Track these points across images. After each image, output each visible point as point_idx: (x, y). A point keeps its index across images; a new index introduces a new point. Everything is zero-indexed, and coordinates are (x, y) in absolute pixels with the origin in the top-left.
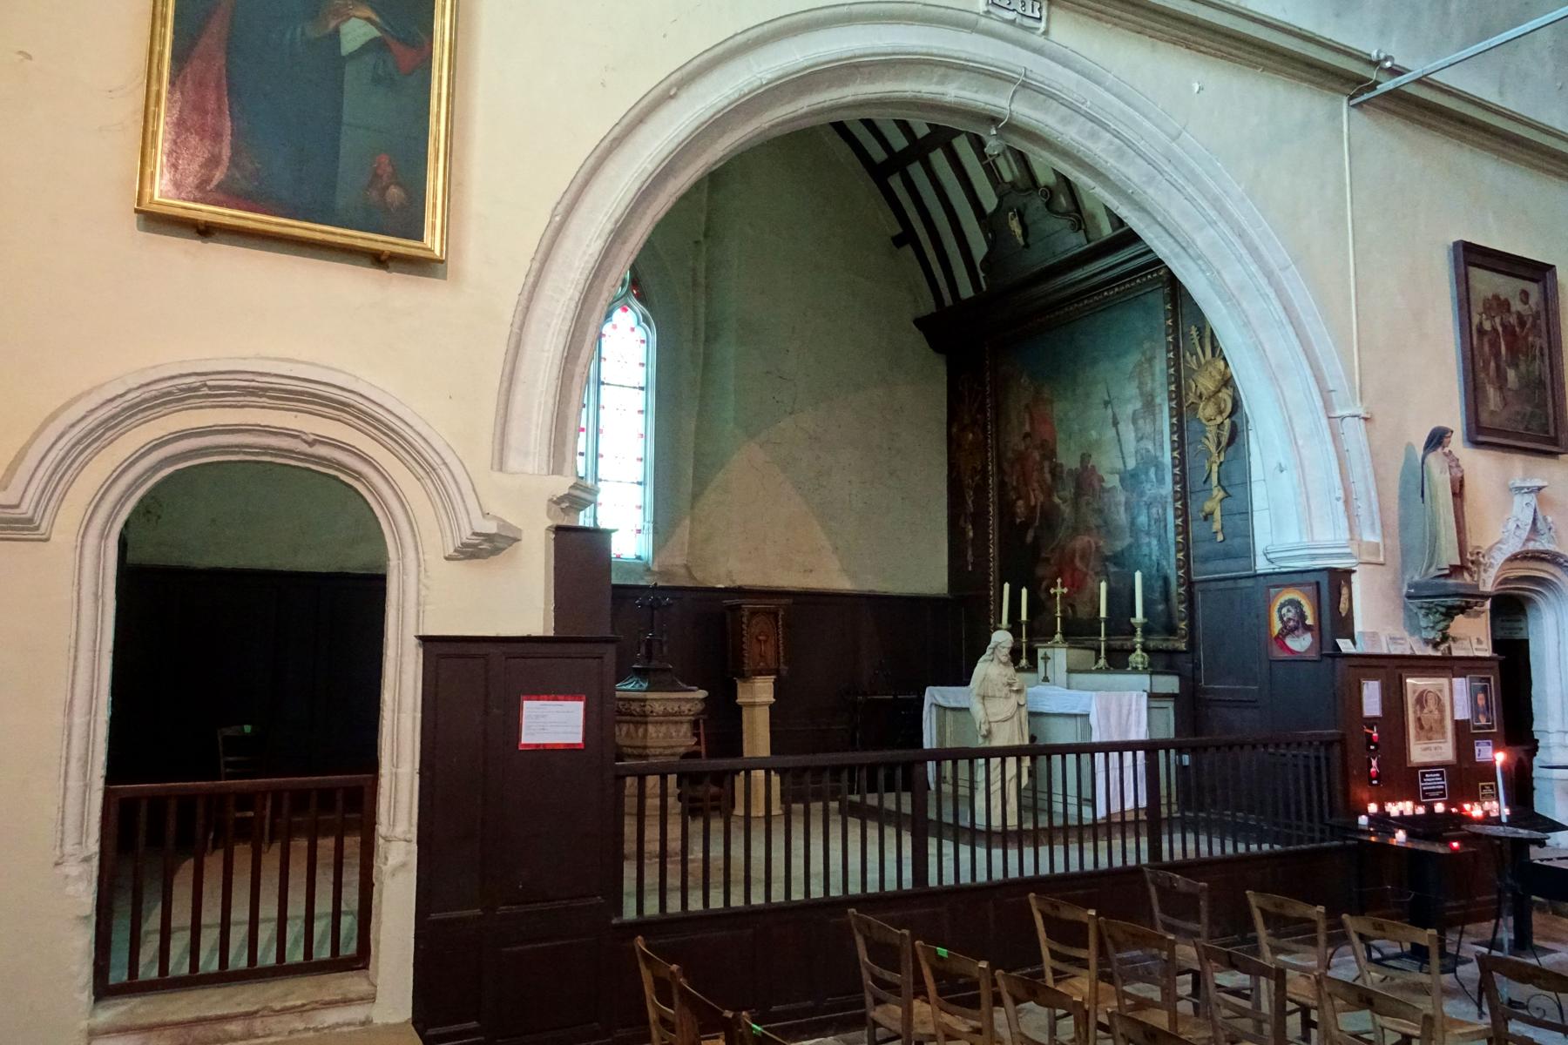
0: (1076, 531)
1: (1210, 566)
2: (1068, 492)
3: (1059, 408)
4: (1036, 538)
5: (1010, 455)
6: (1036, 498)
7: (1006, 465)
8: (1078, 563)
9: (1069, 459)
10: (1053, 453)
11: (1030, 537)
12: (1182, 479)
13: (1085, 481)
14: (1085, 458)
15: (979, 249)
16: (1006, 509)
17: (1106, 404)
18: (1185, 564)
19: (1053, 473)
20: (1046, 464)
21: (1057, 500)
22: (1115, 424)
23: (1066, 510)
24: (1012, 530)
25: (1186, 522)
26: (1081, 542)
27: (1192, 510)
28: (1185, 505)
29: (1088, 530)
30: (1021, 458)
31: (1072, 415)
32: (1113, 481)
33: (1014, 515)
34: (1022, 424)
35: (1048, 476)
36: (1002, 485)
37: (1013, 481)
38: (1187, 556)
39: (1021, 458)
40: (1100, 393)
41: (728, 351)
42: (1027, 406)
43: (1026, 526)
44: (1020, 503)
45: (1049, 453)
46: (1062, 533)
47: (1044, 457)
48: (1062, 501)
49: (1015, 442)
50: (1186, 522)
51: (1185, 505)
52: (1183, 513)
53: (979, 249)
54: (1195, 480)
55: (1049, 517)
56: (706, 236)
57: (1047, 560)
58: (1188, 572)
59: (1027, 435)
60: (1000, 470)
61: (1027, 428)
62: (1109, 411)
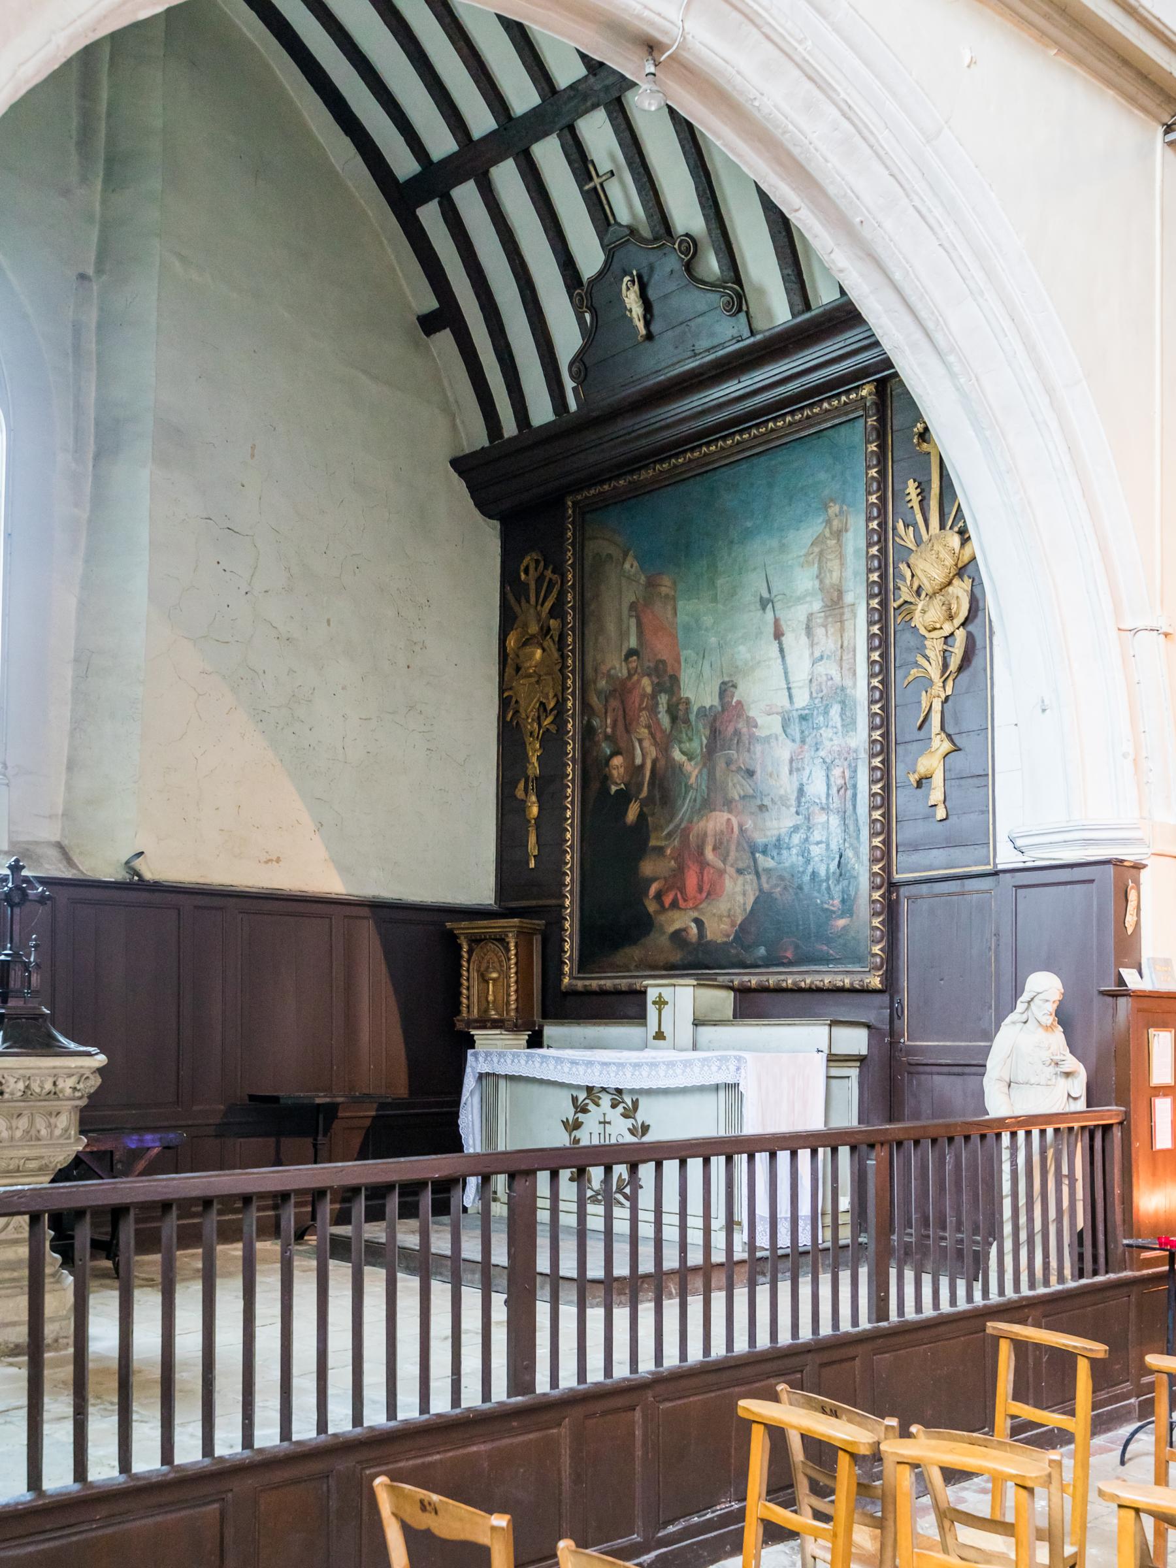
0: (706, 806)
1: (915, 858)
2: (697, 744)
3: (686, 608)
4: (642, 816)
5: (602, 683)
6: (645, 752)
7: (594, 701)
8: (709, 855)
9: (700, 693)
10: (675, 680)
11: (632, 814)
12: (883, 722)
13: (724, 728)
14: (726, 689)
15: (568, 339)
16: (593, 772)
17: (764, 603)
18: (884, 855)
19: (673, 712)
20: (663, 699)
21: (677, 755)
22: (778, 635)
23: (693, 770)
24: (603, 805)
25: (887, 788)
26: (715, 822)
27: (899, 771)
28: (886, 762)
29: (728, 804)
30: (621, 690)
31: (708, 620)
32: (769, 725)
33: (606, 779)
34: (623, 635)
35: (665, 720)
36: (588, 732)
37: (605, 725)
38: (887, 842)
39: (621, 690)
40: (755, 584)
41: (138, 477)
42: (633, 606)
43: (624, 797)
44: (617, 761)
45: (667, 681)
46: (685, 808)
47: (658, 688)
48: (686, 758)
49: (614, 664)
50: (887, 788)
51: (886, 762)
52: (884, 776)
53: (568, 339)
54: (904, 724)
55: (664, 786)
56: (99, 271)
57: (660, 850)
58: (887, 869)
59: (632, 653)
60: (586, 707)
61: (633, 643)
62: (769, 615)
